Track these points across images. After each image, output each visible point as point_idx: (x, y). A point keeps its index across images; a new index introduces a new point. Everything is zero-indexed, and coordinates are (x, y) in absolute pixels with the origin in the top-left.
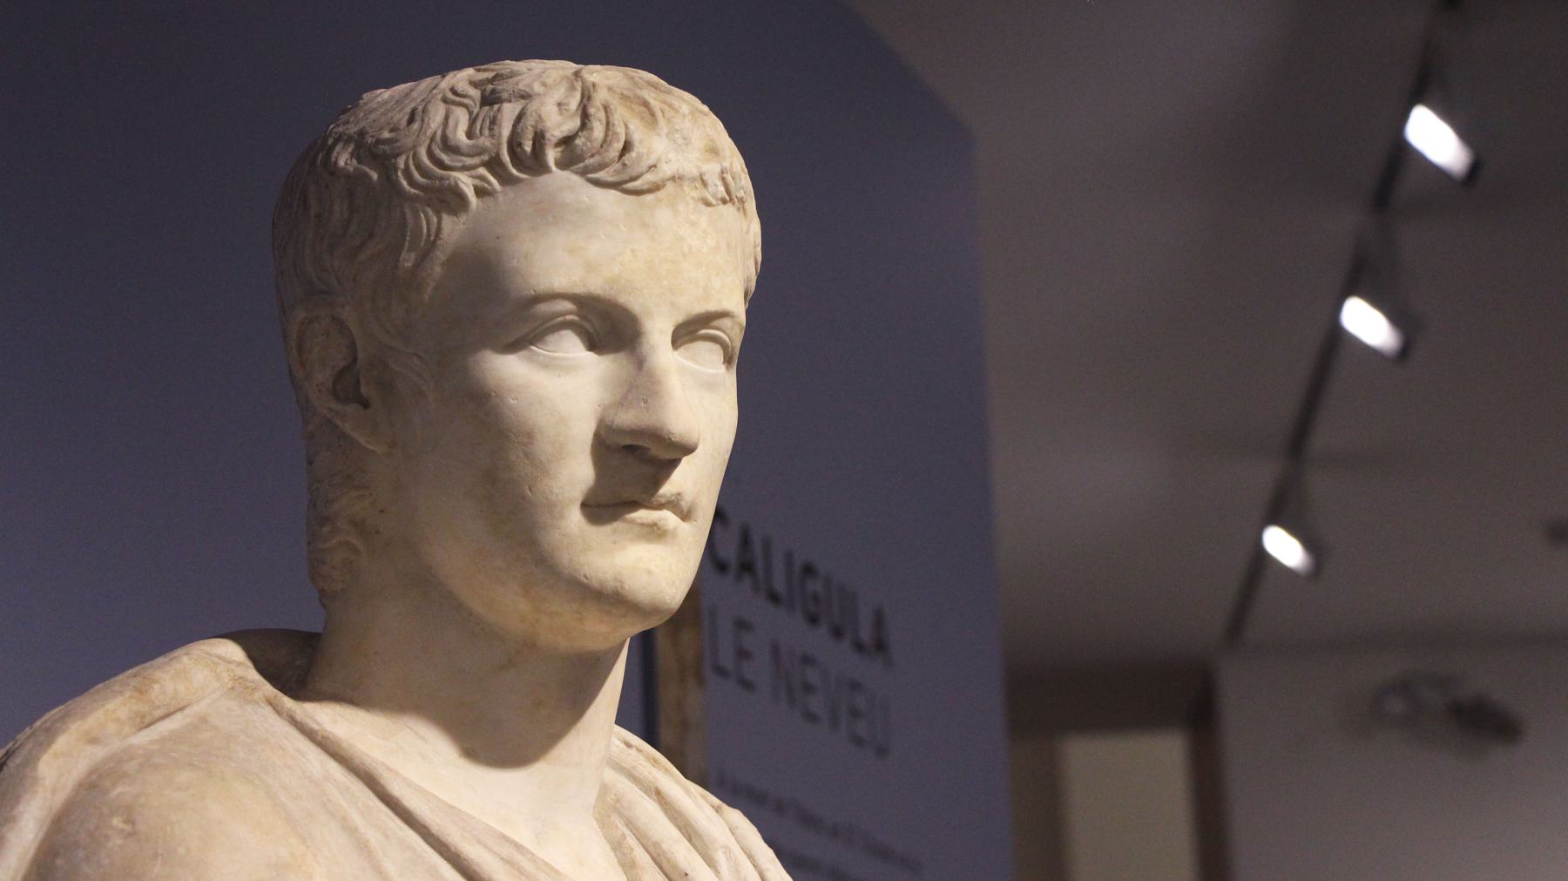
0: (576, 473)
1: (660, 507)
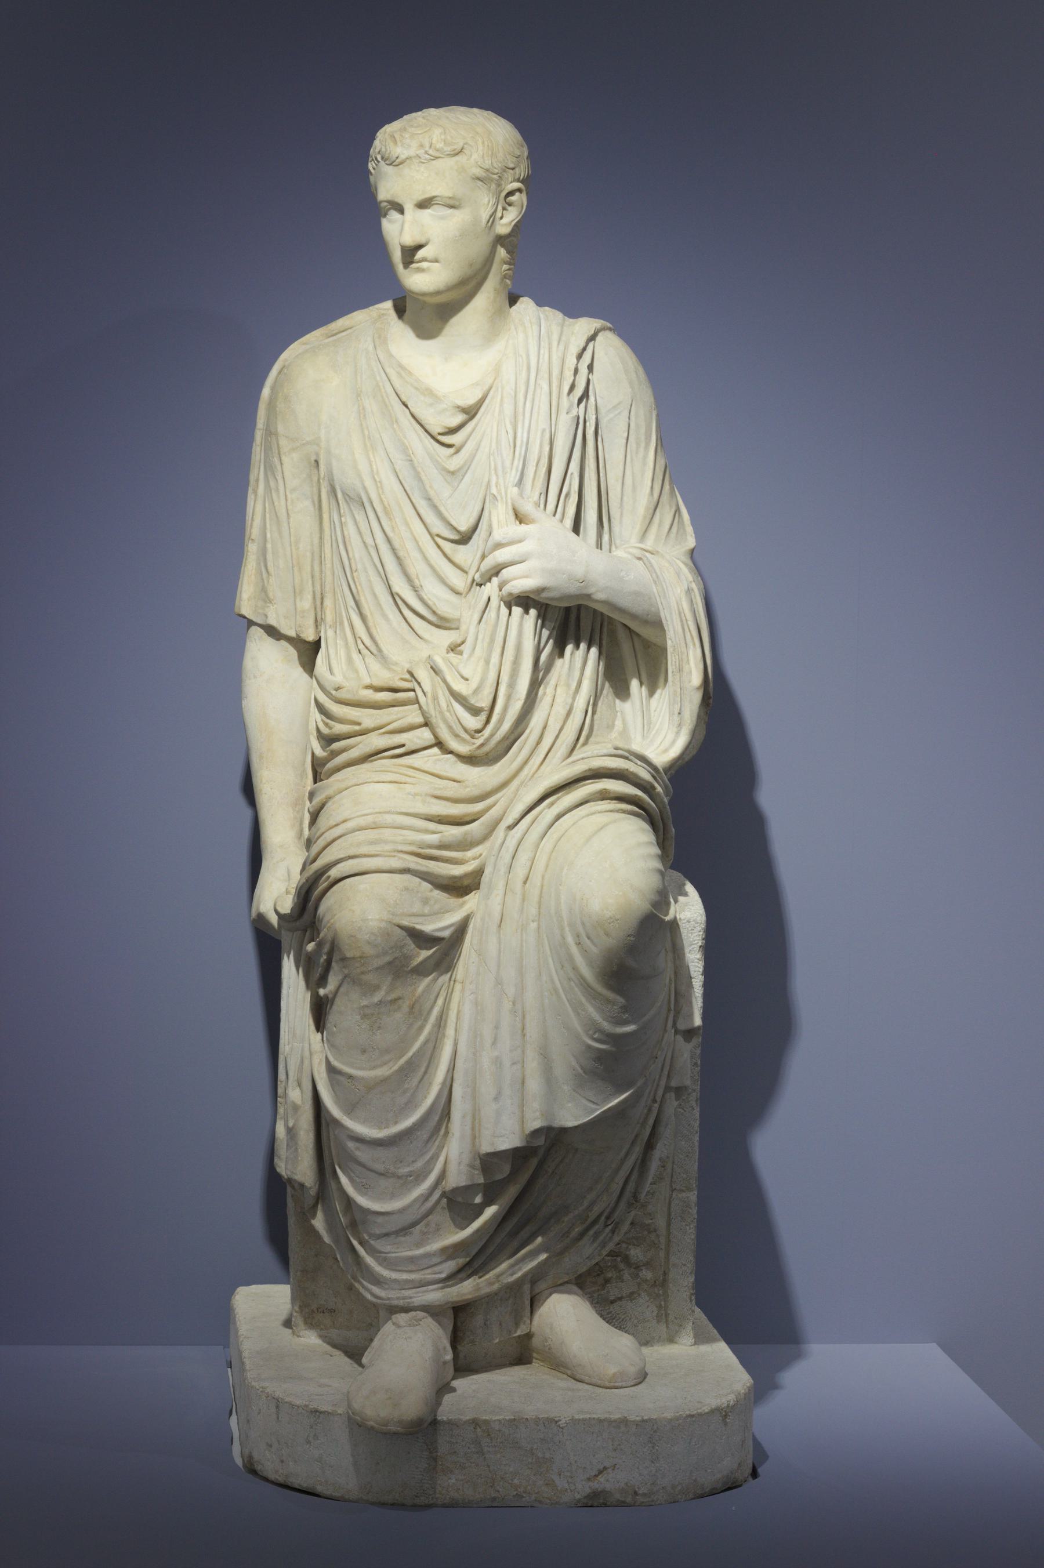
0: (397, 256)
1: (420, 261)
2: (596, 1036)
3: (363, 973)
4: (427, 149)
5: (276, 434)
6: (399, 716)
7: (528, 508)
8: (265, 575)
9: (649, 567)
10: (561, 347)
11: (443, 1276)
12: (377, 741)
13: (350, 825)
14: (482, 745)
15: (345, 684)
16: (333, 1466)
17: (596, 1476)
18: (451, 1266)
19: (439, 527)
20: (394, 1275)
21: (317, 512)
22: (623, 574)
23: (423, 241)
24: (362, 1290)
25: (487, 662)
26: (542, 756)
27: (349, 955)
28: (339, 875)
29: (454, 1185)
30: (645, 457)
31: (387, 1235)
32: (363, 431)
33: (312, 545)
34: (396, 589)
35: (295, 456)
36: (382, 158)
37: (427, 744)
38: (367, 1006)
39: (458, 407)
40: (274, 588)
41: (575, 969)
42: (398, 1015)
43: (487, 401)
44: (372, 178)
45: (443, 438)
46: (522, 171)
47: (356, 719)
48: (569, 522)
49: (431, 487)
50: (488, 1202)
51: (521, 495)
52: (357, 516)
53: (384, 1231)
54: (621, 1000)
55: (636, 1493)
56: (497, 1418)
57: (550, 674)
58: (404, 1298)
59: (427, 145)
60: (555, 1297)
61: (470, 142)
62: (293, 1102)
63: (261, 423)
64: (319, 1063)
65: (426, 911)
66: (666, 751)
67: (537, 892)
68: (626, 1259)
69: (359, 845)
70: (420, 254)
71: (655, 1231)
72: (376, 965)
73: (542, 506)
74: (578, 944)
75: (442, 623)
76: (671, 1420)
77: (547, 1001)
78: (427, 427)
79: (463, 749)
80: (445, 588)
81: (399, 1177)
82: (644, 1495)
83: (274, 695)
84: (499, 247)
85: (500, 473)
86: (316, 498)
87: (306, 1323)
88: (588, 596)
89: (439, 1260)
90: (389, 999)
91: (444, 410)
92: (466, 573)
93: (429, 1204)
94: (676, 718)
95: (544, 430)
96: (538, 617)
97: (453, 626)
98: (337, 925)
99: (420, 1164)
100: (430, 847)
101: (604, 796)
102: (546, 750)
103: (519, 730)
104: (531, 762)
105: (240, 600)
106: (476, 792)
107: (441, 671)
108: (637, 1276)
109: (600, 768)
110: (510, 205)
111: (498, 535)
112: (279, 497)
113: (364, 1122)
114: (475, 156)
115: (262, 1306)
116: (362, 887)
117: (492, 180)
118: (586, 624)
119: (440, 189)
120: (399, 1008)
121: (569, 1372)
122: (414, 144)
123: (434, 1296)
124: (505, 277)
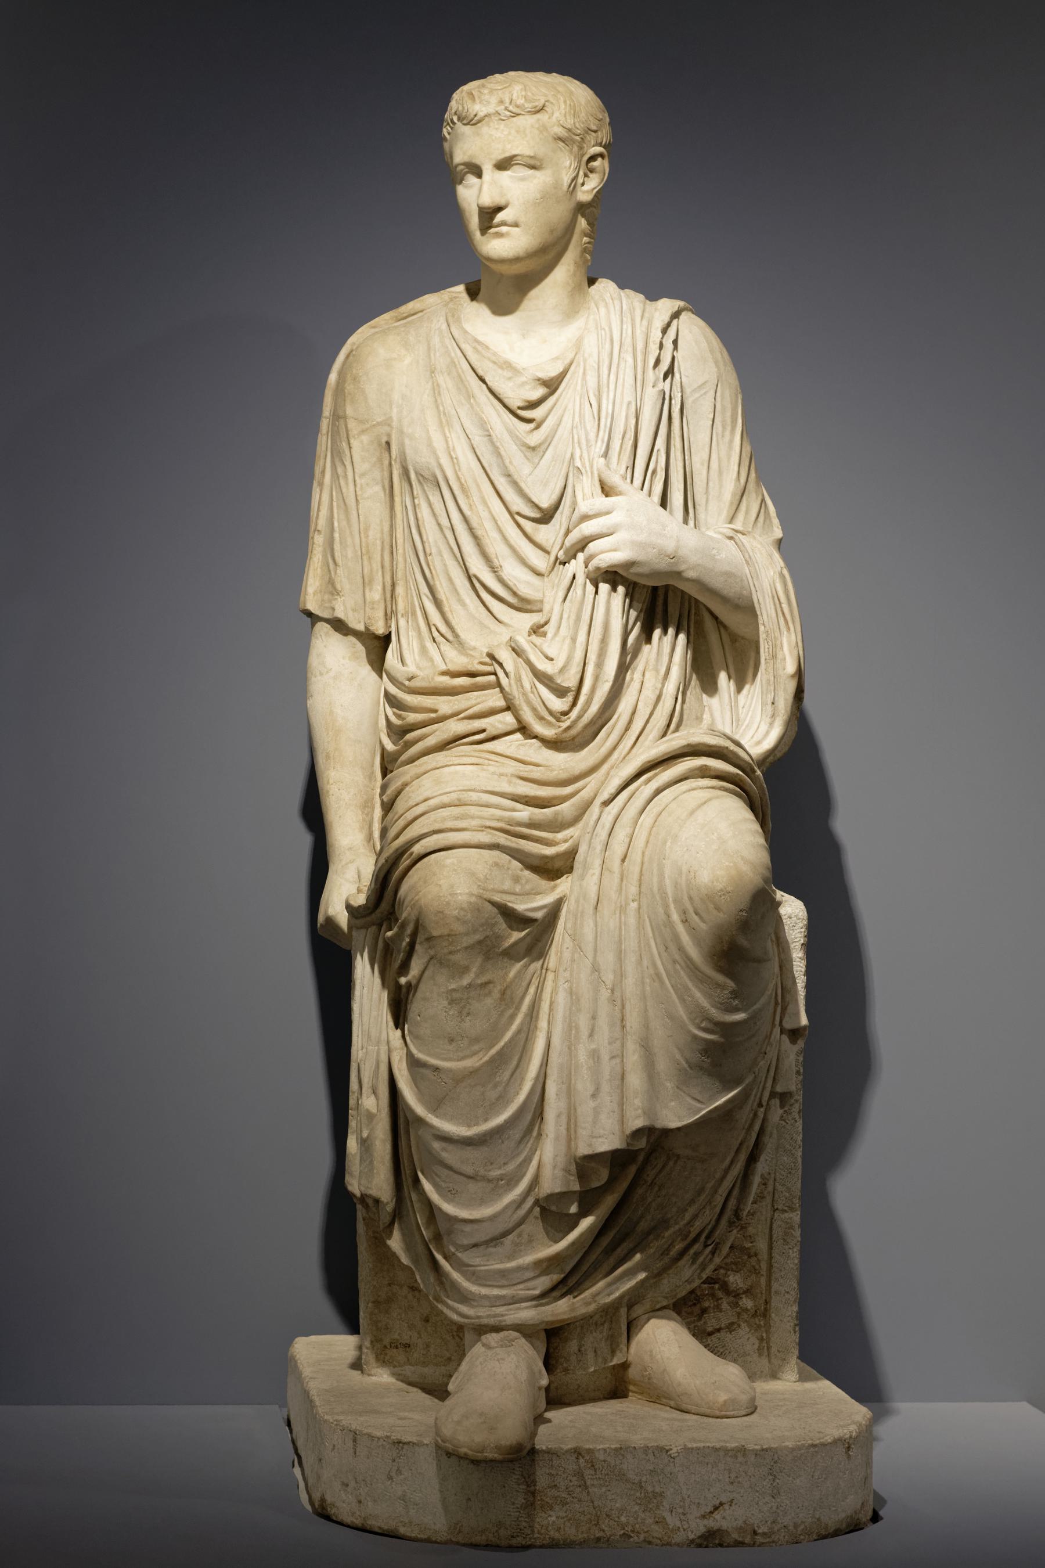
0: (474, 221)
1: (498, 226)
2: (703, 1025)
3: (450, 953)
4: (507, 105)
5: (345, 417)
6: (479, 700)
7: (615, 479)
8: (332, 566)
9: (740, 546)
10: (645, 323)
11: (537, 1292)
12: (455, 727)
13: (432, 803)
14: (569, 728)
15: (418, 673)
16: (422, 1503)
17: (711, 1513)
18: (544, 1282)
19: (518, 504)
20: (484, 1291)
21: (388, 499)
23: (502, 202)
24: (446, 1310)
25: (574, 640)
26: (634, 739)
27: (435, 933)
28: (423, 851)
29: (549, 1192)
30: (731, 441)
31: (475, 1245)
32: (437, 407)
33: (382, 533)
34: (473, 570)
35: (365, 438)
36: (459, 119)
37: (509, 728)
38: (454, 990)
39: (539, 379)
40: (342, 580)
41: (681, 949)
42: (489, 1001)
43: (568, 376)
44: (446, 145)
45: (523, 412)
46: (605, 135)
47: (432, 706)
48: (657, 497)
49: (511, 462)
50: (583, 1213)
51: (608, 465)
52: (431, 497)
53: (473, 1241)
54: (731, 984)
55: (755, 1533)
56: (601, 1446)
57: (638, 659)
58: (495, 1316)
59: (507, 101)
60: (653, 1322)
61: (551, 100)
62: (367, 1110)
63: (327, 410)
64: (400, 1060)
65: (518, 889)
66: (759, 743)
67: (637, 869)
68: (725, 1287)
69: (444, 820)
70: (500, 217)
71: (756, 1255)
72: (465, 945)
73: (629, 480)
74: (685, 921)
75: (523, 605)
76: (793, 1449)
77: (648, 988)
78: (506, 401)
79: (548, 732)
80: (526, 570)
81: (489, 1181)
82: (764, 1534)
83: (343, 693)
84: (580, 217)
85: (584, 447)
86: (387, 483)
87: (377, 1359)
88: (679, 574)
89: (532, 1275)
90: (479, 982)
91: (524, 384)
92: (548, 553)
93: (522, 1212)
94: (769, 708)
95: (629, 403)
96: (626, 595)
97: (535, 608)
98: (422, 902)
99: (511, 1167)
100: (520, 824)
101: (704, 773)
102: (637, 733)
103: (607, 715)
104: (621, 747)
105: (306, 594)
106: (564, 776)
107: (523, 651)
108: (736, 1305)
109: (699, 744)
110: (592, 171)
111: (583, 507)
112: (347, 484)
113: (451, 1119)
114: (557, 114)
115: (324, 1355)
116: (448, 861)
117: (574, 141)
118: (674, 609)
119: (521, 147)
120: (490, 992)
121: (672, 1403)
122: (494, 100)
123: (526, 1314)
124: (585, 250)
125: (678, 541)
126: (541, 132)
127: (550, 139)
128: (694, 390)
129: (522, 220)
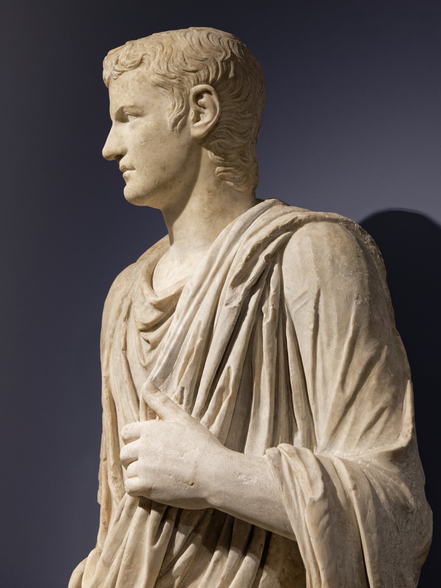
22: (242, 477)
70: (123, 163)
117: (172, 84)
125: (196, 467)
126: (140, 82)
127: (150, 87)
128: (295, 301)
129: (135, 163)
